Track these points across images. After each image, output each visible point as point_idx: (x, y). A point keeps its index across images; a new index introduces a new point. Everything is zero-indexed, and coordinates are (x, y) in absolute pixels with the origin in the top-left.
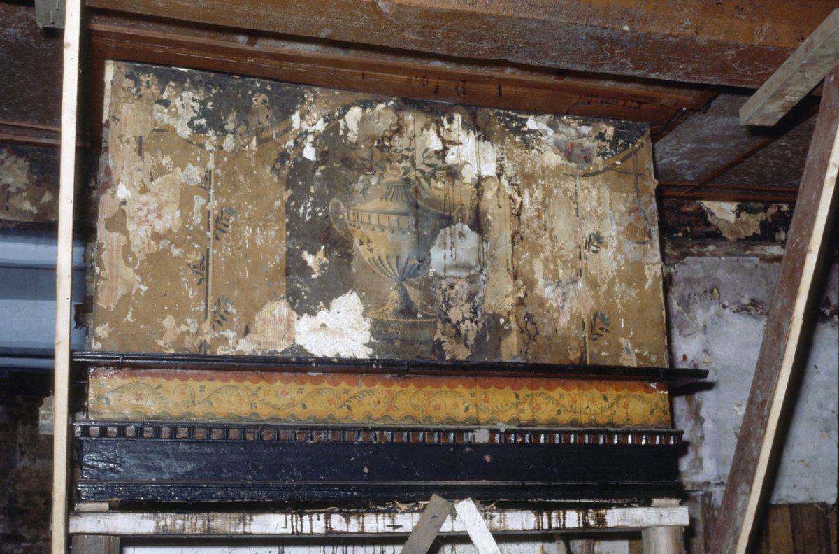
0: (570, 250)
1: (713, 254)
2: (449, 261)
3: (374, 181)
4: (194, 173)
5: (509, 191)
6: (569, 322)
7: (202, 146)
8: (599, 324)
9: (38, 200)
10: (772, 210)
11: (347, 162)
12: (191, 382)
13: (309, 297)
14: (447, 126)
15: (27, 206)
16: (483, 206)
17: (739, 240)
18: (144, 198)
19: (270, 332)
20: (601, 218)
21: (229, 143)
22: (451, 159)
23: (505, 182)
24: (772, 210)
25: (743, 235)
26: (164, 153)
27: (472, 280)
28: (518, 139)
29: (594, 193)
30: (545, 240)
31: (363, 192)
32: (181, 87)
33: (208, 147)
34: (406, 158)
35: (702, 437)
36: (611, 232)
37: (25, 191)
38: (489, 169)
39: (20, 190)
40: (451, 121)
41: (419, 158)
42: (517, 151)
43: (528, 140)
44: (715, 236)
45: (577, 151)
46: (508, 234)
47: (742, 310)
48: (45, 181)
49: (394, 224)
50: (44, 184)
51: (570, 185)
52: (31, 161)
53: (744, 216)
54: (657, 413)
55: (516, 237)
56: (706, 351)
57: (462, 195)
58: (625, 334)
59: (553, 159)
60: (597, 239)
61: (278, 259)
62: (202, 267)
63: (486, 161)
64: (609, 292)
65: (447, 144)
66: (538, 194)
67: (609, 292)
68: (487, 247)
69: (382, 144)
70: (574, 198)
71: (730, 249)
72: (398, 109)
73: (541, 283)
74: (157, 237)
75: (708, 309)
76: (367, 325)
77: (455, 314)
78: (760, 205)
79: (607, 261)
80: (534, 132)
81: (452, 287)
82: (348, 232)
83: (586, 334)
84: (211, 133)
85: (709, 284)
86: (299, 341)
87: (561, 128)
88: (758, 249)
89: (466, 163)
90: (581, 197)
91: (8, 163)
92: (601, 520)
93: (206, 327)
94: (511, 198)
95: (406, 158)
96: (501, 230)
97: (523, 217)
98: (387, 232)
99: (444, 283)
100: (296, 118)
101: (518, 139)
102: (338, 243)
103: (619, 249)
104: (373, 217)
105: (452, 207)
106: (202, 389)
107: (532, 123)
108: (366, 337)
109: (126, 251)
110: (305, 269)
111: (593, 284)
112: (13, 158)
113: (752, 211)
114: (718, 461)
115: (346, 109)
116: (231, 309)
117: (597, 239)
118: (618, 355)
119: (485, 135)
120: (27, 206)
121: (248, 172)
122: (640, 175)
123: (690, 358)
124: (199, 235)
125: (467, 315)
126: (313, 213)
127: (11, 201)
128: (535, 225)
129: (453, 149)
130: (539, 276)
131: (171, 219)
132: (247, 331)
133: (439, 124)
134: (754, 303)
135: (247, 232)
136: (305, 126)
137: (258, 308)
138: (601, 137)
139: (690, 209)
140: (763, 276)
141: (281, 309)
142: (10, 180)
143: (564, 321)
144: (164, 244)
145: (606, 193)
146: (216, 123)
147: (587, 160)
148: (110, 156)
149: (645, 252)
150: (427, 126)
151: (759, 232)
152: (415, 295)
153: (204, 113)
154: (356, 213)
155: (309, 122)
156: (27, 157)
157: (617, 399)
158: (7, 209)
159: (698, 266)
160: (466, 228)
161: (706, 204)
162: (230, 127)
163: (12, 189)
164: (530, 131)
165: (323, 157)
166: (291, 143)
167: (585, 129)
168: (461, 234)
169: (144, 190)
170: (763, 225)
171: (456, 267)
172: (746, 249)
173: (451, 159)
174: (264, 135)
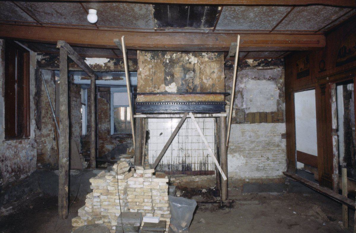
0: (209, 74)
1: (248, 69)
2: (189, 77)
3: (177, 65)
4: (151, 66)
5: (199, 65)
6: (208, 85)
7: (152, 62)
8: (213, 85)
10: (260, 60)
11: (174, 63)
12: (151, 96)
13: (167, 83)
14: (189, 55)
15: (132, 68)
16: (195, 68)
17: (253, 66)
18: (144, 70)
19: (162, 89)
20: (214, 69)
21: (156, 61)
22: (190, 61)
23: (198, 64)
24: (260, 60)
25: (254, 65)
26: (146, 63)
27: (193, 80)
28: (201, 57)
29: (213, 64)
30: (205, 73)
31: (176, 67)
32: (148, 53)
33: (152, 62)
34: (182, 61)
35: (243, 101)
36: (216, 71)
38: (196, 62)
40: (190, 54)
41: (185, 61)
42: (201, 59)
43: (203, 57)
44: (249, 66)
45: (211, 58)
46: (199, 72)
47: (252, 79)
49: (181, 72)
51: (209, 64)
52: (133, 61)
53: (255, 62)
54: (222, 99)
55: (200, 72)
56: (245, 86)
57: (191, 66)
58: (217, 87)
59: (207, 59)
60: (214, 72)
61: (163, 78)
62: (152, 80)
63: (196, 61)
64: (215, 81)
65: (189, 58)
66: (204, 65)
67: (215, 81)
68: (195, 74)
69: (179, 59)
70: (210, 66)
71: (251, 68)
72: (181, 53)
73: (204, 79)
74: (145, 76)
75: (246, 79)
76: (176, 87)
77: (190, 85)
78: (258, 60)
79: (215, 76)
80: (204, 55)
81: (189, 81)
82: (174, 73)
83: (211, 87)
84: (153, 60)
85: (246, 75)
86: (166, 90)
87: (208, 54)
88: (257, 68)
89: (192, 61)
90: (211, 65)
92: (212, 115)
93: (153, 88)
94: (199, 66)
95: (182, 61)
96: (198, 72)
97: (201, 69)
98: (180, 73)
99: (188, 80)
100: (166, 56)
101: (201, 57)
102: (172, 76)
103: (217, 73)
104: (177, 71)
105: (190, 68)
106: (153, 97)
107: (203, 54)
108: (176, 89)
109: (141, 78)
110: (167, 79)
111: (213, 79)
113: (256, 61)
114: (246, 105)
115: (173, 54)
116: (156, 86)
117: (214, 72)
118: (216, 90)
119: (196, 56)
120: (132, 68)
121: (159, 65)
122: (221, 61)
123: (242, 88)
124: (152, 75)
125: (192, 85)
126: (168, 71)
128: (203, 70)
129: (190, 59)
130: (204, 79)
131: (148, 73)
132: (159, 89)
133: (188, 55)
134: (255, 77)
135: (158, 74)
136: (167, 57)
137: (160, 85)
138: (215, 55)
139: (244, 61)
140: (257, 73)
141: (163, 85)
143: (207, 85)
144: (147, 77)
145: (215, 64)
146: (154, 58)
147: (212, 59)
149: (222, 74)
150: (186, 56)
151: (257, 64)
152: (184, 82)
153: (152, 57)
154: (175, 70)
155: (167, 57)
157: (216, 97)
159: (244, 72)
160: (192, 72)
161: (247, 60)
162: (156, 58)
164: (203, 55)
165: (170, 62)
166: (165, 60)
167: (212, 54)
168: (191, 73)
169: (143, 69)
170: (258, 63)
171: (190, 78)
172: (255, 68)
173: (190, 61)
174: (161, 59)
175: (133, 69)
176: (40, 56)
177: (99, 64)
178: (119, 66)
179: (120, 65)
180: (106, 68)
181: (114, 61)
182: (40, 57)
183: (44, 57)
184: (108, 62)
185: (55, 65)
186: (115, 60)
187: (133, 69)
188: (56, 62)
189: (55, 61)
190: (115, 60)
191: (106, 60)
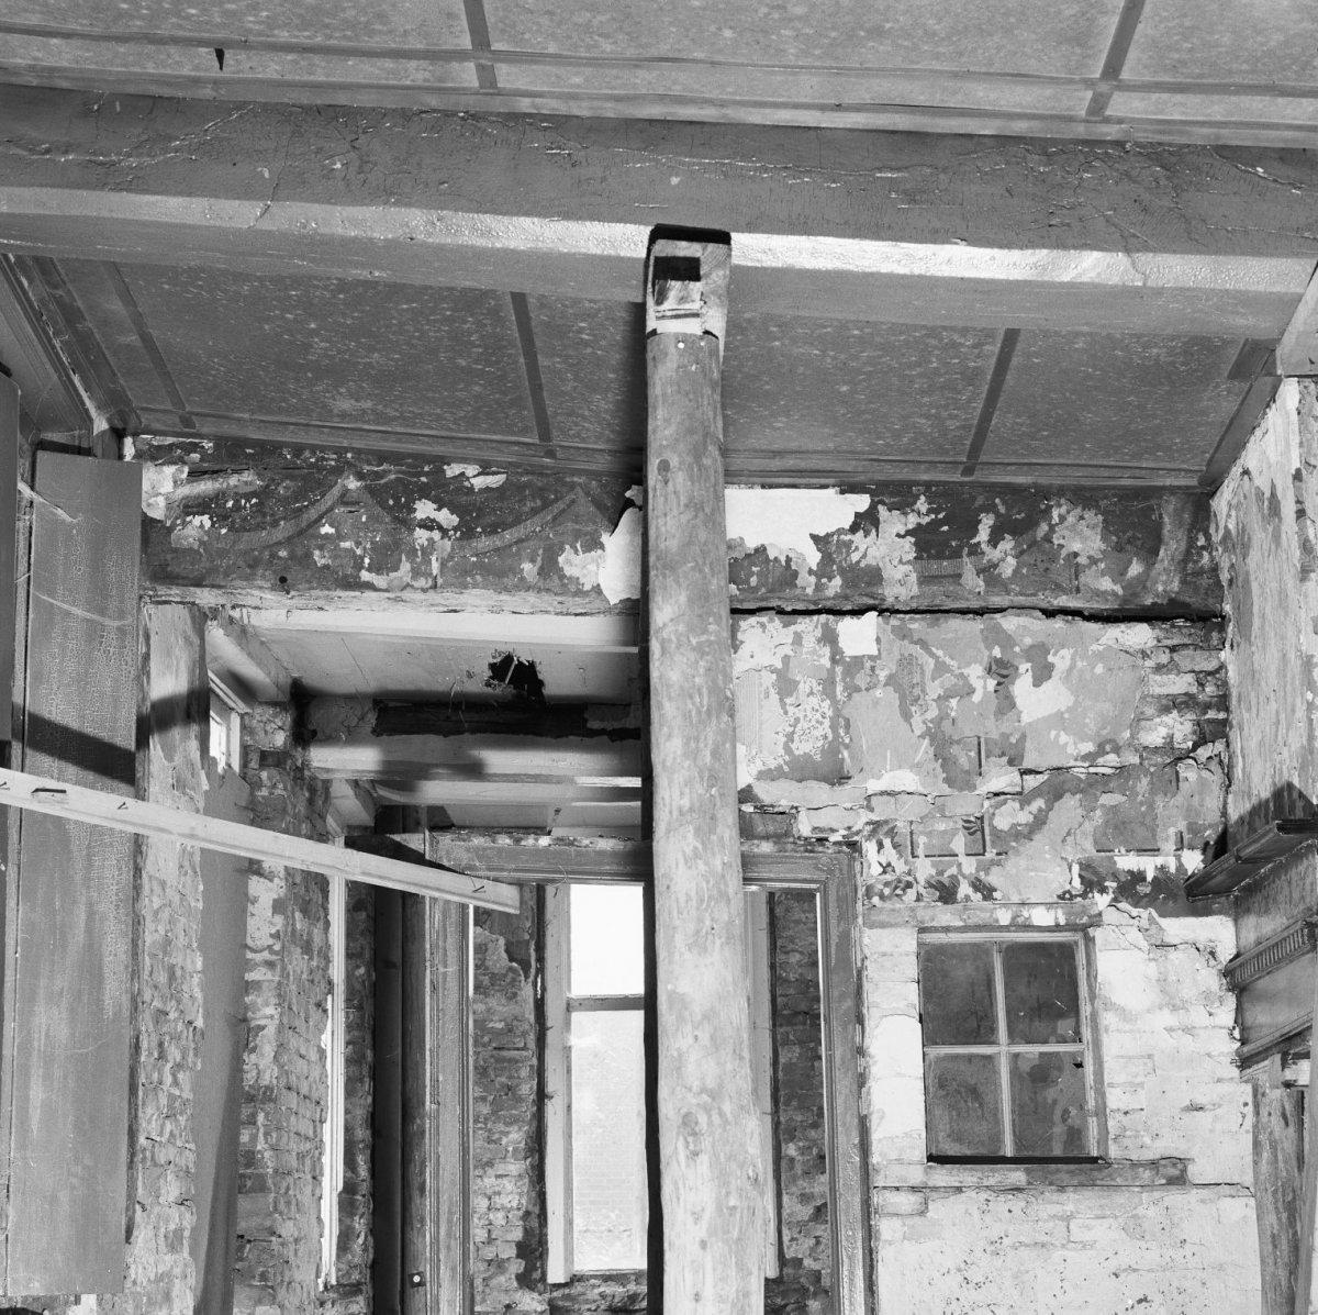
9: (1123, 573)
15: (1106, 584)
37: (1101, 560)
39: (1093, 561)
48: (1129, 542)
50: (1129, 547)
91: (1071, 519)
112: (1079, 510)
120: (1106, 584)
127: (1082, 579)
142: (1076, 546)
148: (1309, 522)
156: (1097, 507)
158: (1078, 590)
163: (1082, 560)
175: (1118, 589)
176: (169, 470)
177: (761, 550)
178: (968, 566)
179: (975, 551)
180: (837, 581)
181: (912, 521)
182: (167, 487)
183: (206, 487)
184: (854, 529)
185: (319, 558)
186: (922, 504)
187: (1118, 589)
188: (327, 529)
189: (317, 522)
190: (922, 504)
191: (835, 509)
